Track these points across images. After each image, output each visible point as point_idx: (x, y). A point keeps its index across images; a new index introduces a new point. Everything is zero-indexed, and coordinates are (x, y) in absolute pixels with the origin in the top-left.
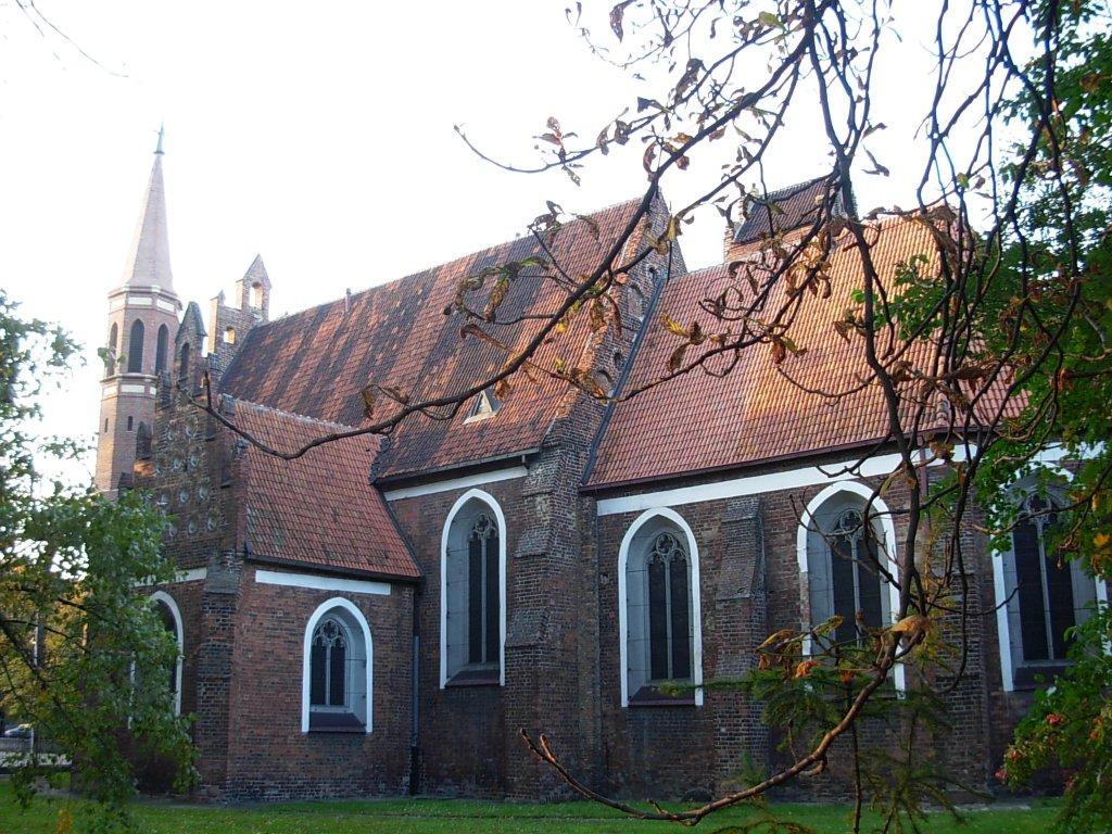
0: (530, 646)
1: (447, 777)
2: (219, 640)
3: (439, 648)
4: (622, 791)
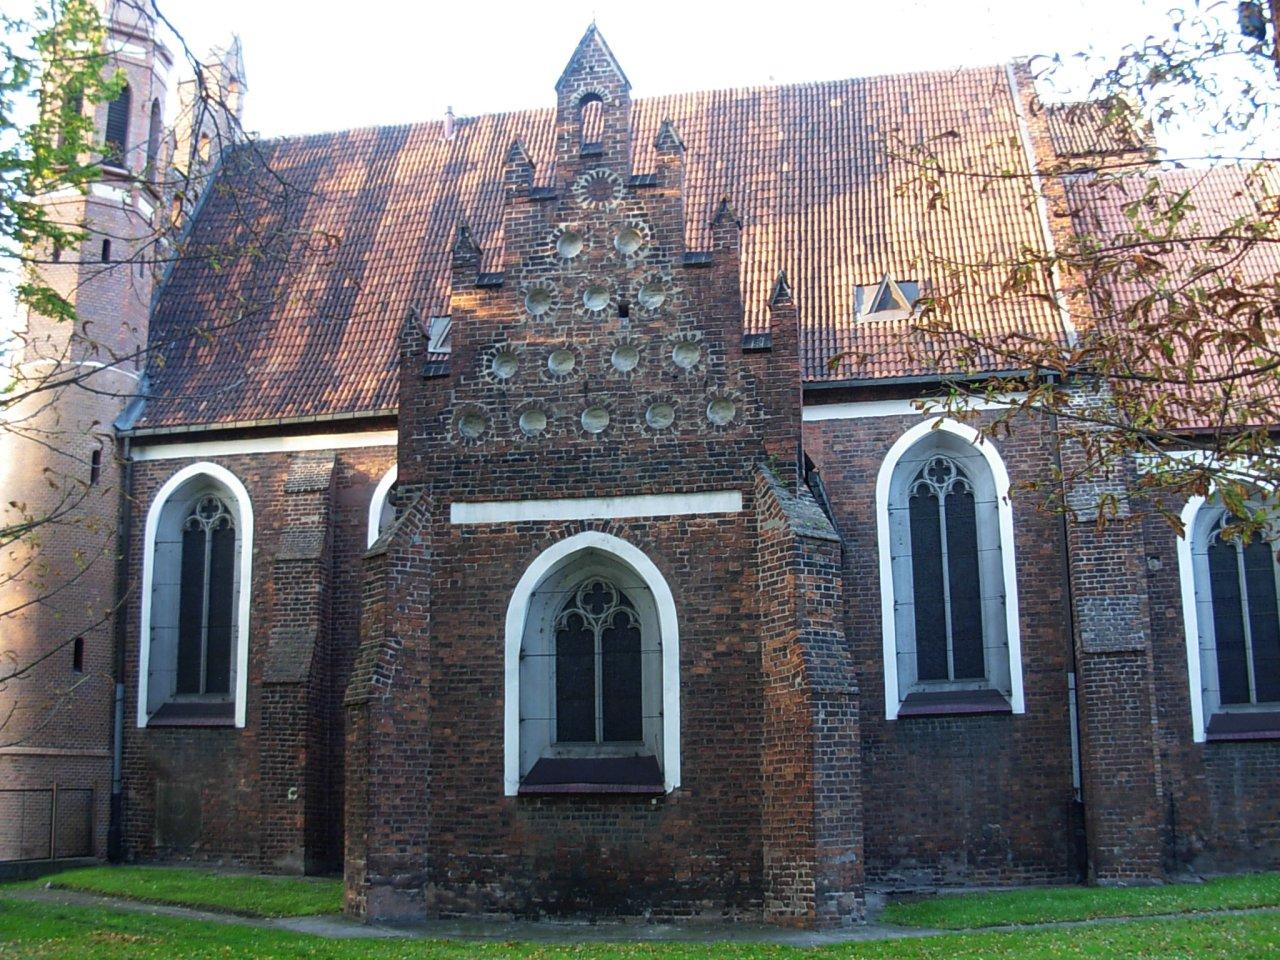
0: (1135, 652)
1: (909, 856)
2: (823, 624)
3: (881, 657)
4: (1199, 861)
